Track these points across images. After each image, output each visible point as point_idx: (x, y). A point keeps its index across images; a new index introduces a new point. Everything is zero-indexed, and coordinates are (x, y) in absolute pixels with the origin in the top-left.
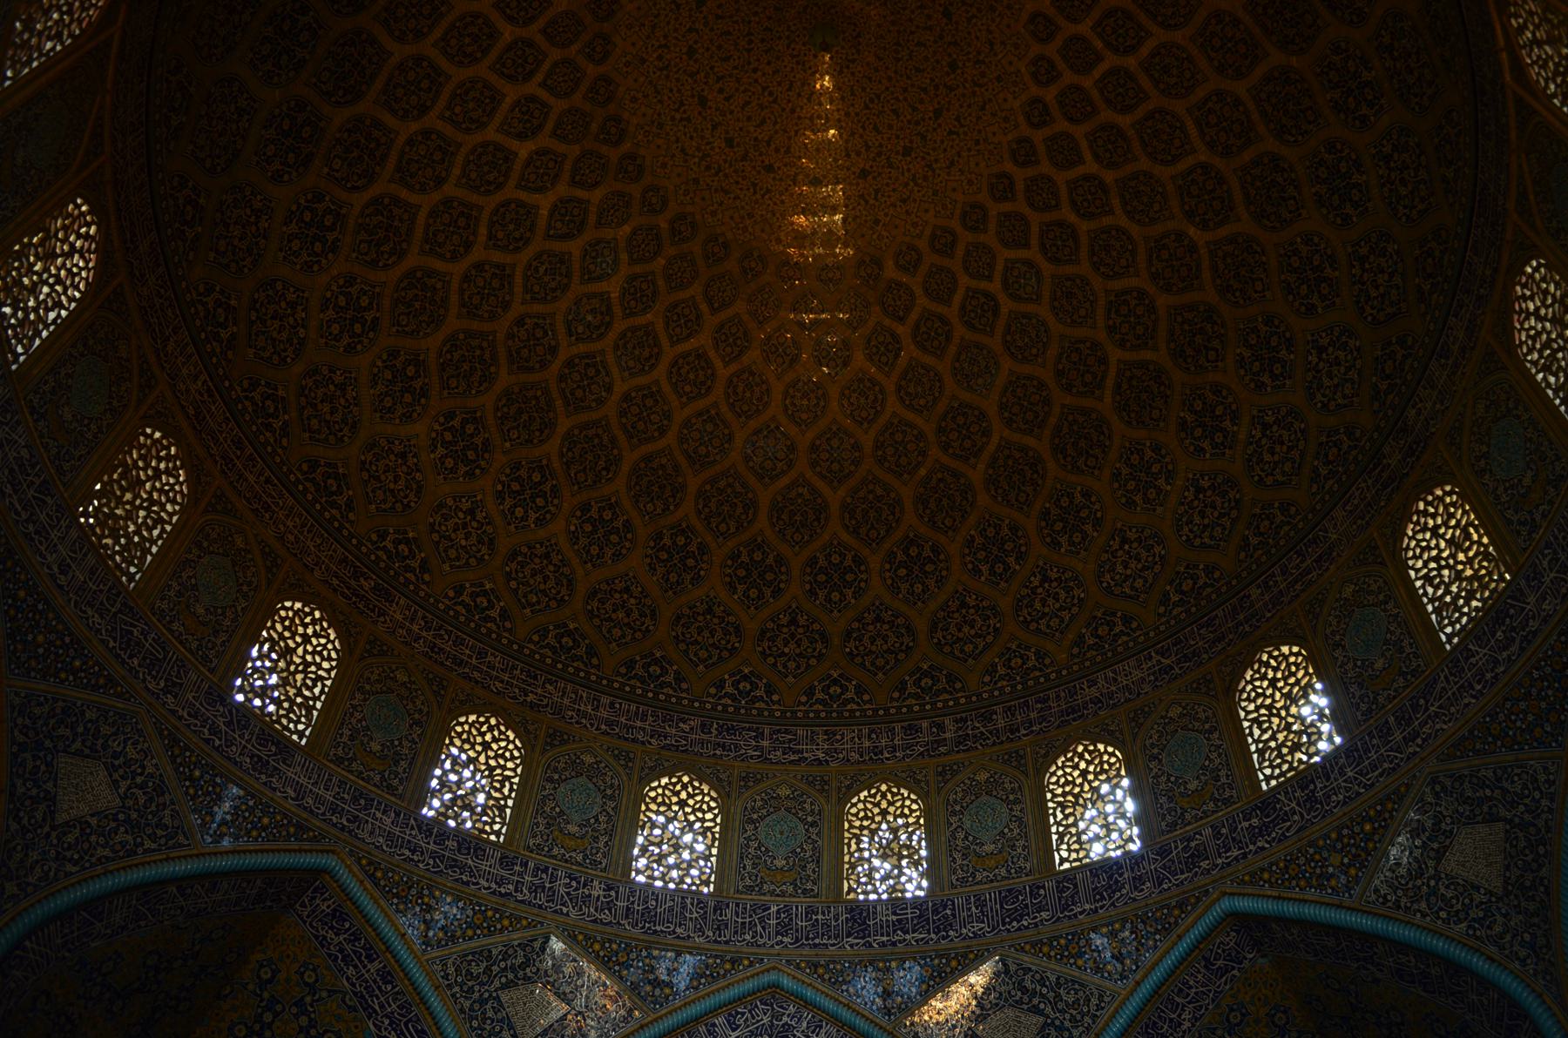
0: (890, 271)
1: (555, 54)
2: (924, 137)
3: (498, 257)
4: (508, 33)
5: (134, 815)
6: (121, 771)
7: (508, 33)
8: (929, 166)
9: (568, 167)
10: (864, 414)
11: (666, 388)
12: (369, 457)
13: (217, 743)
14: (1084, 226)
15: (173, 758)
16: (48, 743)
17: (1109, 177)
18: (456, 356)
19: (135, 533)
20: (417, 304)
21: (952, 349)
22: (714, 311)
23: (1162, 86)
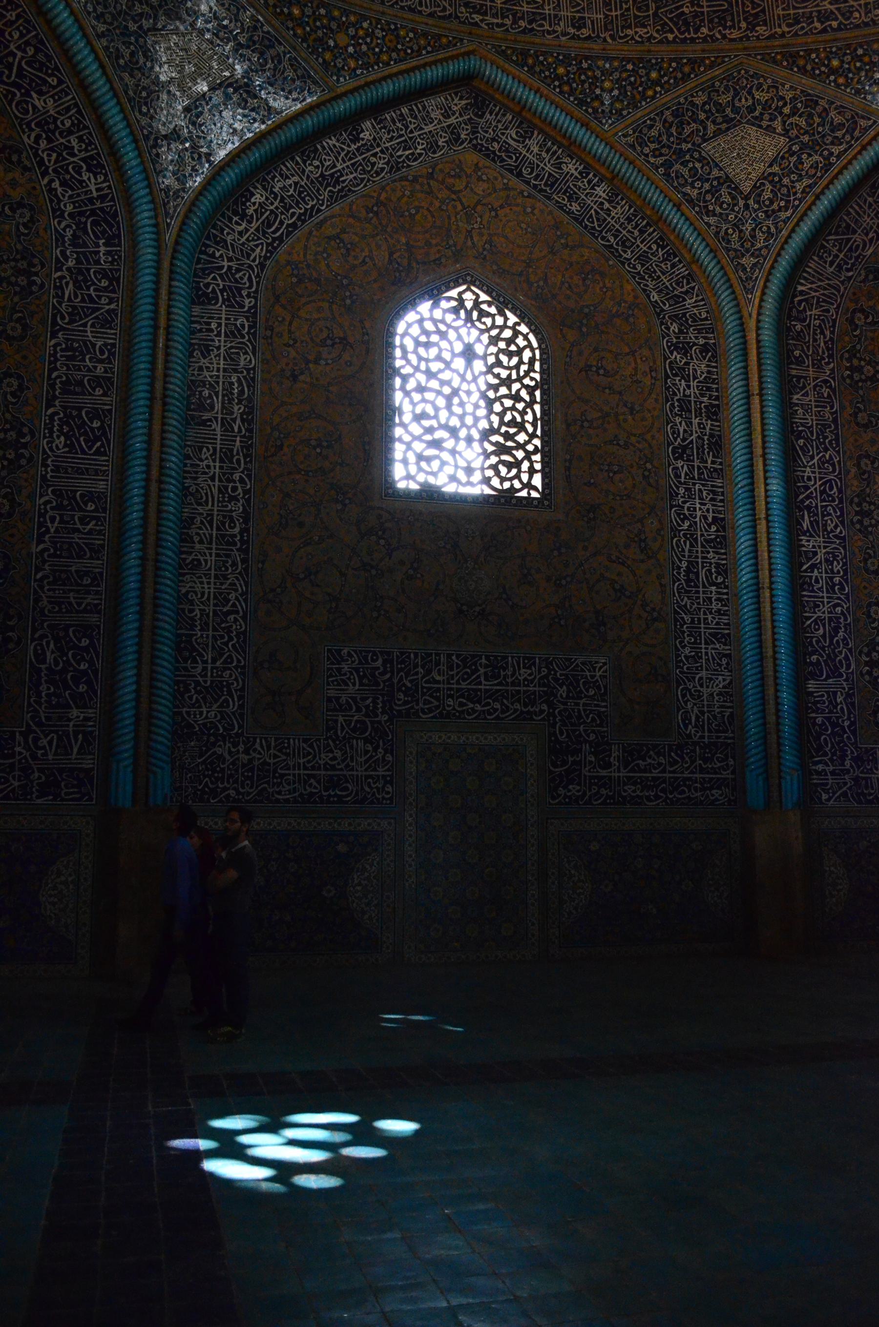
5: (806, 138)
6: (766, 117)
13: (835, 24)
15: (803, 70)
16: (684, 146)
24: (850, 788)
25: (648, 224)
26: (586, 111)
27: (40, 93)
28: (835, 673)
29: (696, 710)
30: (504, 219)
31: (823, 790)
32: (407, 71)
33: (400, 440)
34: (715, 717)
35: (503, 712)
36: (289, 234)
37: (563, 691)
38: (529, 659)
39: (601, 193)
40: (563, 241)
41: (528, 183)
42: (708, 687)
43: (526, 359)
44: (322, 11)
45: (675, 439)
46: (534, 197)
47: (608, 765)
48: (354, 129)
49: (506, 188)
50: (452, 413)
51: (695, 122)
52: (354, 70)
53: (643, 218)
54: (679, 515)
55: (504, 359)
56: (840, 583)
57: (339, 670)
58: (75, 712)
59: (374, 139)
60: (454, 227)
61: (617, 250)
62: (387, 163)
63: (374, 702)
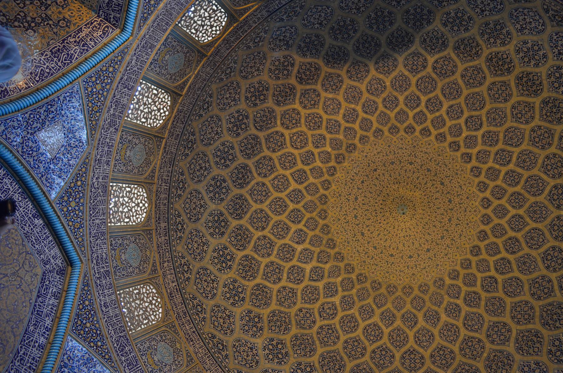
0: (448, 281)
1: (308, 215)
2: (447, 231)
3: (291, 285)
4: (291, 206)
7: (291, 206)
8: (452, 239)
9: (316, 255)
10: (452, 338)
11: (363, 338)
12: (237, 344)
14: (519, 235)
17: (521, 212)
18: (275, 319)
19: (137, 316)
20: (260, 297)
21: (483, 303)
22: (379, 308)
23: (526, 168)
25: (34, 370)
26: (75, 319)
30: (17, 292)
32: (68, 234)
39: (41, 340)
40: (15, 326)
41: (36, 302)
44: (81, 195)
46: (30, 306)
48: (38, 216)
49: (31, 291)
51: (88, 370)
52: (63, 211)
53: (36, 366)
59: (36, 225)
60: (7, 267)
61: (18, 357)
62: (27, 232)
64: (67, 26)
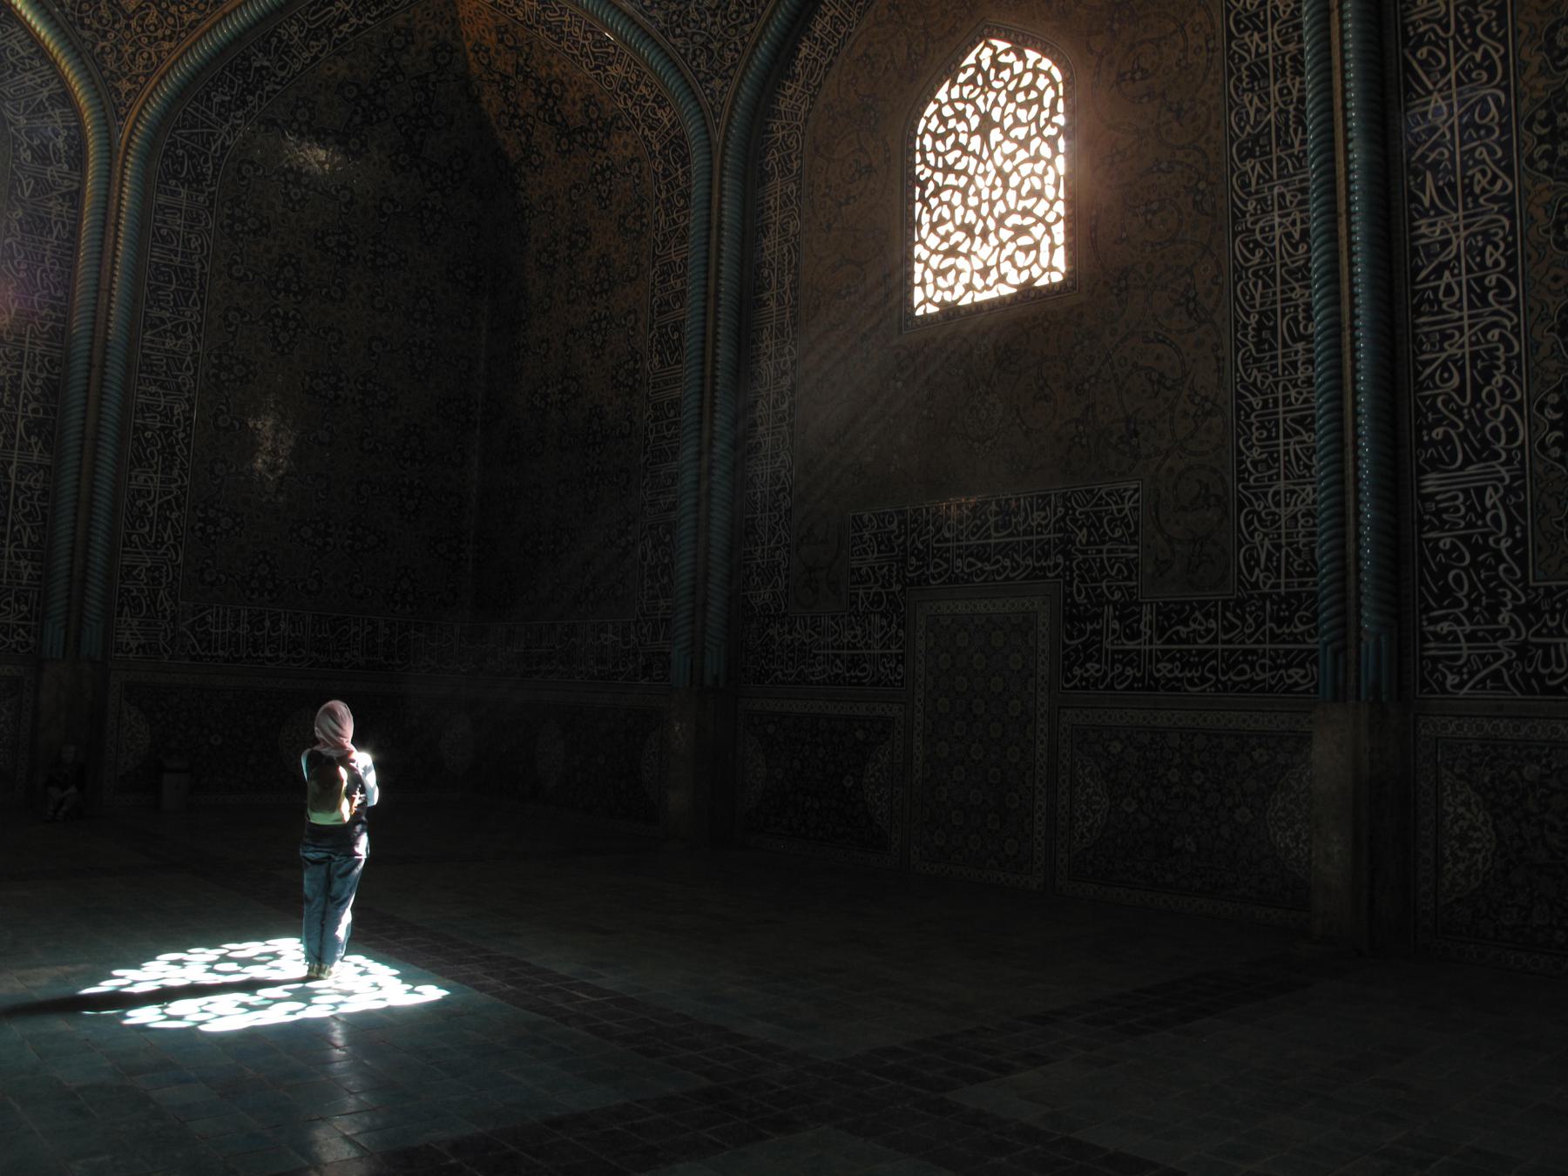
24: (1508, 665)
27: (610, 64)
28: (1484, 452)
29: (1267, 543)
31: (1450, 669)
33: (919, 260)
34: (1298, 552)
35: (1014, 569)
36: (826, 73)
37: (1082, 535)
38: (1043, 497)
42: (1287, 505)
43: (1047, 103)
45: (1242, 129)
47: (1135, 635)
50: (966, 207)
54: (1246, 245)
55: (1022, 114)
56: (1500, 282)
57: (861, 537)
58: (662, 602)
63: (890, 570)
64: (507, 31)
